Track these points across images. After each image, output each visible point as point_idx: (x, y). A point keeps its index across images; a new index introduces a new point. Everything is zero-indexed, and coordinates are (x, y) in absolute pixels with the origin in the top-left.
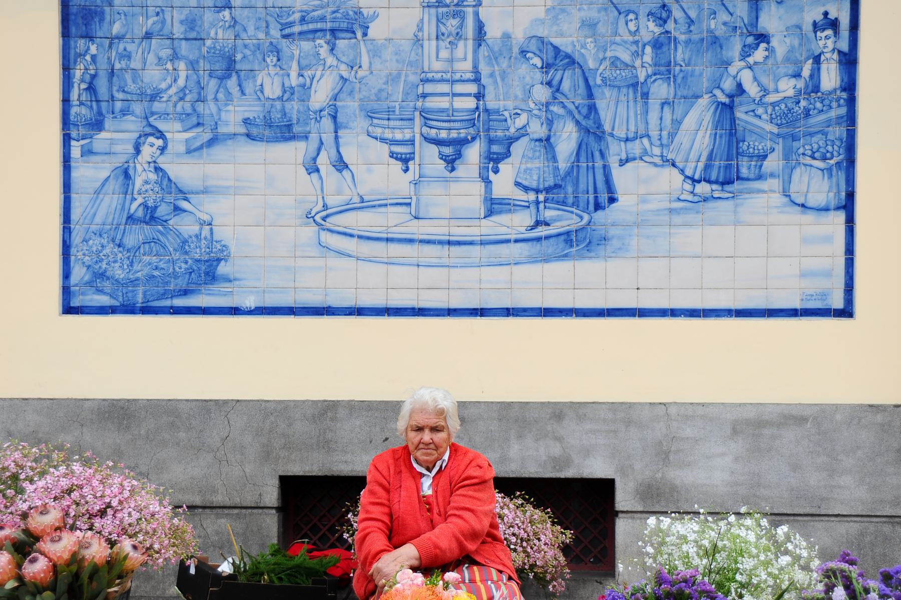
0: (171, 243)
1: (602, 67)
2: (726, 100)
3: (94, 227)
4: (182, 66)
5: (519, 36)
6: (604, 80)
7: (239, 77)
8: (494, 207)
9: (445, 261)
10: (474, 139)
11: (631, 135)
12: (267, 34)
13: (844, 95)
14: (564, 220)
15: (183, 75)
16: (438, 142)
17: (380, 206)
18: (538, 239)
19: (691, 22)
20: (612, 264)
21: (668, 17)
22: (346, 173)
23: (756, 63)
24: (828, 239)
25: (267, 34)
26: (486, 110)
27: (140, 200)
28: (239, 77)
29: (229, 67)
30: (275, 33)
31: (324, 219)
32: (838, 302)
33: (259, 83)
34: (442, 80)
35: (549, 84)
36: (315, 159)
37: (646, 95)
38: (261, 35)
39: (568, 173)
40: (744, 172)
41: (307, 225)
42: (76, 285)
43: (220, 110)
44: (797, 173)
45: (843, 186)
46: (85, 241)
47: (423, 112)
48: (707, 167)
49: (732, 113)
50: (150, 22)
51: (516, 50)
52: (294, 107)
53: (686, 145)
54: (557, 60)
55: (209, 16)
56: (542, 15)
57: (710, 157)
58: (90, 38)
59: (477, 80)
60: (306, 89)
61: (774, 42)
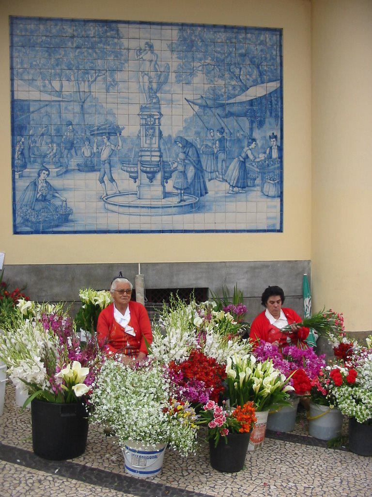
0: (52, 209)
1: (202, 148)
2: (243, 160)
3: (24, 203)
4: (55, 145)
5: (174, 136)
6: (203, 152)
7: (75, 149)
8: (166, 195)
9: (150, 214)
10: (159, 171)
11: (212, 171)
12: (85, 134)
13: (279, 160)
14: (190, 200)
15: (55, 148)
16: (146, 172)
17: (126, 194)
18: (182, 206)
19: (231, 134)
20: (206, 214)
21: (224, 132)
22: (113, 183)
23: (252, 148)
24: (275, 207)
25: (85, 134)
26: (163, 161)
27: (40, 193)
28: (75, 149)
29: (71, 145)
30: (88, 134)
31: (106, 199)
32: (278, 228)
33: (83, 151)
34: (148, 151)
35: (184, 153)
36: (103, 178)
37: (217, 158)
38: (84, 135)
39: (191, 184)
40: (249, 184)
41: (100, 201)
42: (18, 224)
43: (68, 161)
44: (265, 185)
45: (279, 190)
46: (21, 208)
47: (141, 161)
48: (237, 182)
49: (245, 164)
50: (43, 130)
51: (173, 141)
52: (95, 160)
53: (230, 175)
54: (187, 145)
55: (64, 128)
56: (182, 130)
57: (238, 179)
58: (22, 135)
59: (160, 151)
60: (99, 153)
61: (258, 142)
